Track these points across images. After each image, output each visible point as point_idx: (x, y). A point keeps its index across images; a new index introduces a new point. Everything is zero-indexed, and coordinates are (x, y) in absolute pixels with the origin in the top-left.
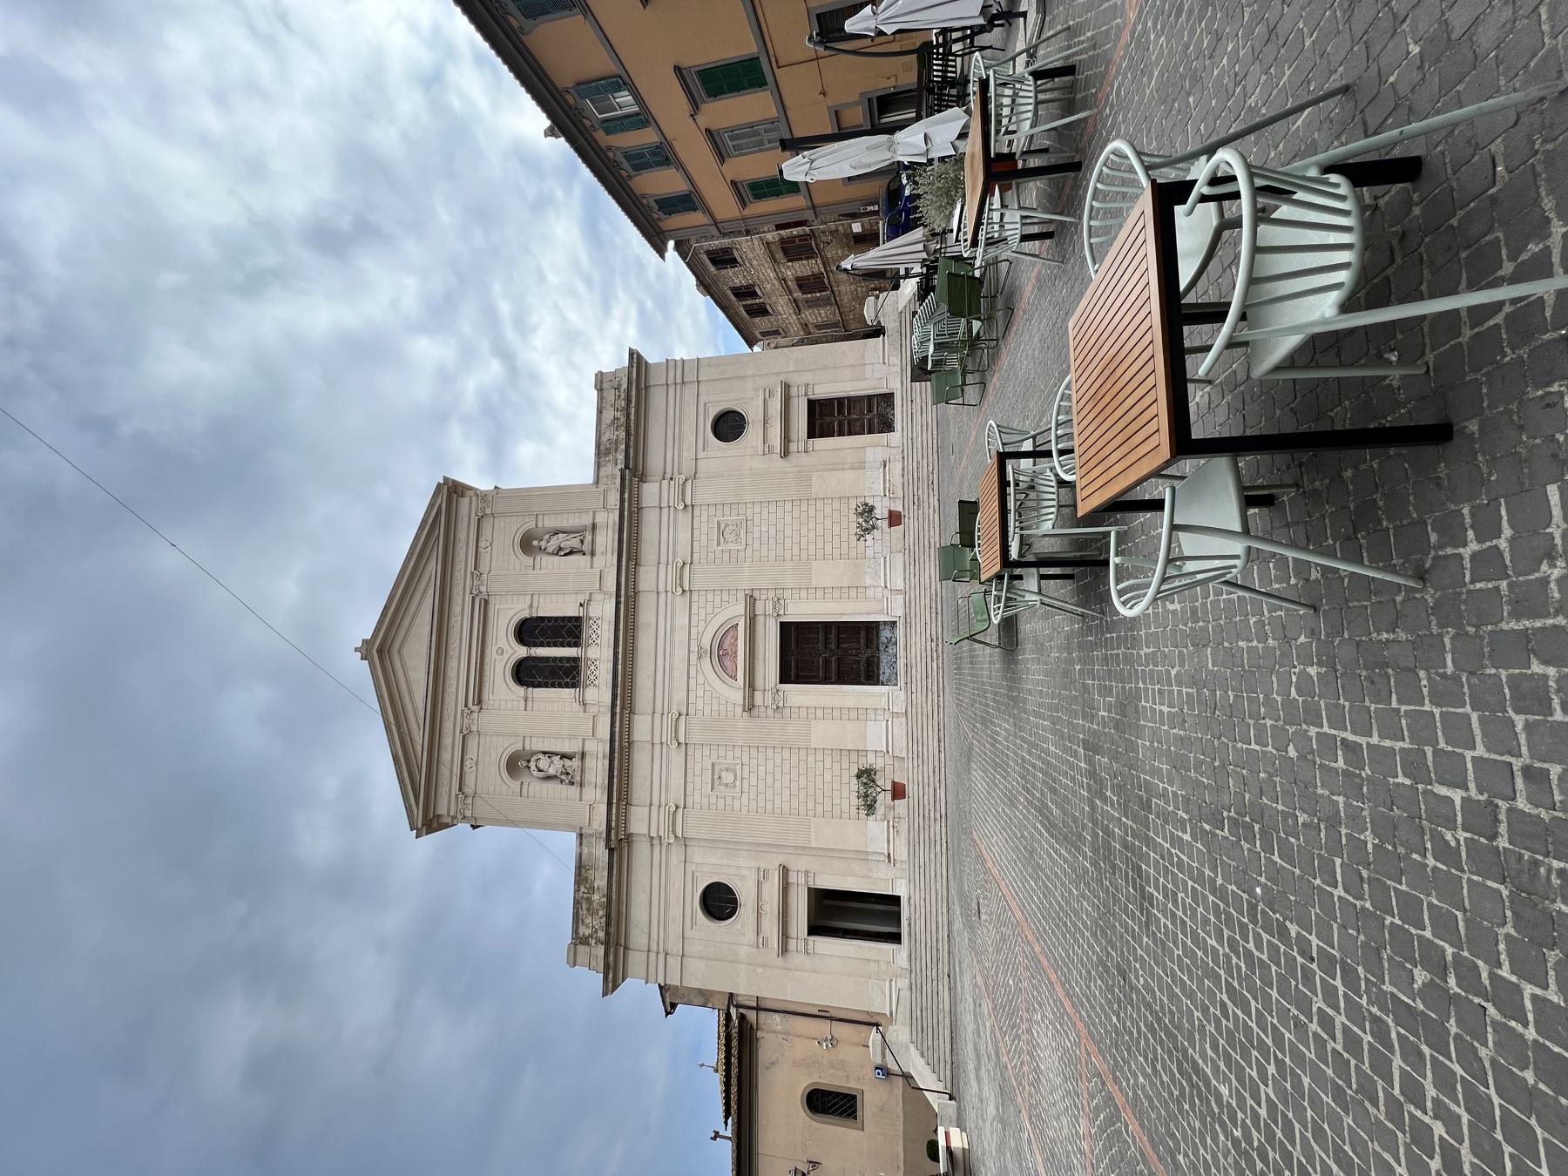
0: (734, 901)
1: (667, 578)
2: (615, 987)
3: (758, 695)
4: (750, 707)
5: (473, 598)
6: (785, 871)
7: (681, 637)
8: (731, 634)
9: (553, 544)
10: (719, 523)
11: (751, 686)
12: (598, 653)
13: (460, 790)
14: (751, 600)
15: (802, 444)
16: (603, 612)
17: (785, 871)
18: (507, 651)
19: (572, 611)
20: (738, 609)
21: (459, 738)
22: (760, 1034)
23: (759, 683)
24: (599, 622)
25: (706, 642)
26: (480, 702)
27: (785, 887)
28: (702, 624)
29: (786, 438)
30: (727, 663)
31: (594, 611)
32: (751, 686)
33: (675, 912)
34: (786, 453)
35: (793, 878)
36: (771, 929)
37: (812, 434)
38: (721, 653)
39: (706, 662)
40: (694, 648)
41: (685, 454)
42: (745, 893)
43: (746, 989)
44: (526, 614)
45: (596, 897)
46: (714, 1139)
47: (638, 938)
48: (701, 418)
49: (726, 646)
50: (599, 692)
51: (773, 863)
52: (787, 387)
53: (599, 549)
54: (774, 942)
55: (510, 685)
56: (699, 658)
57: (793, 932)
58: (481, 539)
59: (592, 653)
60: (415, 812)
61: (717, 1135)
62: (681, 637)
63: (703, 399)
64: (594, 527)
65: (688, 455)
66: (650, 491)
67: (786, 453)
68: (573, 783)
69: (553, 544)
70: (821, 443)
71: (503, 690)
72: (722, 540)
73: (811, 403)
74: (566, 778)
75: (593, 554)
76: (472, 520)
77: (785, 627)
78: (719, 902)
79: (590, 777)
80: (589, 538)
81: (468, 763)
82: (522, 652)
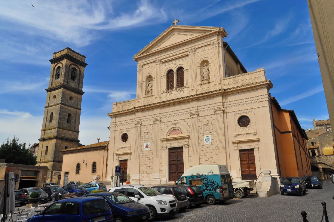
0: (125, 141)
1: (194, 110)
2: (109, 116)
3: (165, 142)
4: (163, 140)
5: (188, 51)
6: (131, 154)
7: (179, 118)
8: (181, 132)
9: (204, 70)
10: (210, 124)
11: (167, 140)
12: (176, 94)
13: (143, 65)
14: (189, 137)
15: (235, 148)
16: (184, 93)
17: (131, 154)
18: (174, 66)
19: (185, 83)
20: (185, 134)
21: (154, 60)
22: (104, 150)
23: (168, 142)
24: (182, 92)
25: (177, 125)
26: (163, 63)
27: (127, 154)
28: (181, 123)
29: (238, 143)
30: (174, 132)
31: (185, 90)
32: (167, 140)
33: (123, 127)
34: (234, 143)
35: (129, 155)
36: (122, 151)
37: (240, 151)
38: (175, 130)
39: (173, 126)
40: (177, 122)
41: (233, 108)
42: (127, 144)
43: (110, 147)
44: (185, 69)
45: (125, 107)
46: (98, 139)
47: (118, 119)
48: (246, 111)
49: (177, 131)
50: (165, 97)
51: (132, 151)
52: (258, 141)
53: (203, 86)
54: (119, 152)
55: (166, 72)
56: (174, 124)
57: (120, 157)
58: (205, 47)
59: (174, 92)
60: (138, 55)
61: (99, 139)
62: (179, 118)
63: (253, 110)
64: (209, 83)
65: (233, 109)
66: (219, 99)
67: (234, 143)
68: (146, 95)
69: (204, 70)
70: (237, 154)
71: (165, 68)
72: (205, 125)
73: (252, 150)
74: (147, 92)
75: (201, 85)
76: (209, 42)
77: (182, 148)
78: (125, 138)
79: (147, 99)
80: (206, 82)
81: (149, 64)
82: (175, 71)
